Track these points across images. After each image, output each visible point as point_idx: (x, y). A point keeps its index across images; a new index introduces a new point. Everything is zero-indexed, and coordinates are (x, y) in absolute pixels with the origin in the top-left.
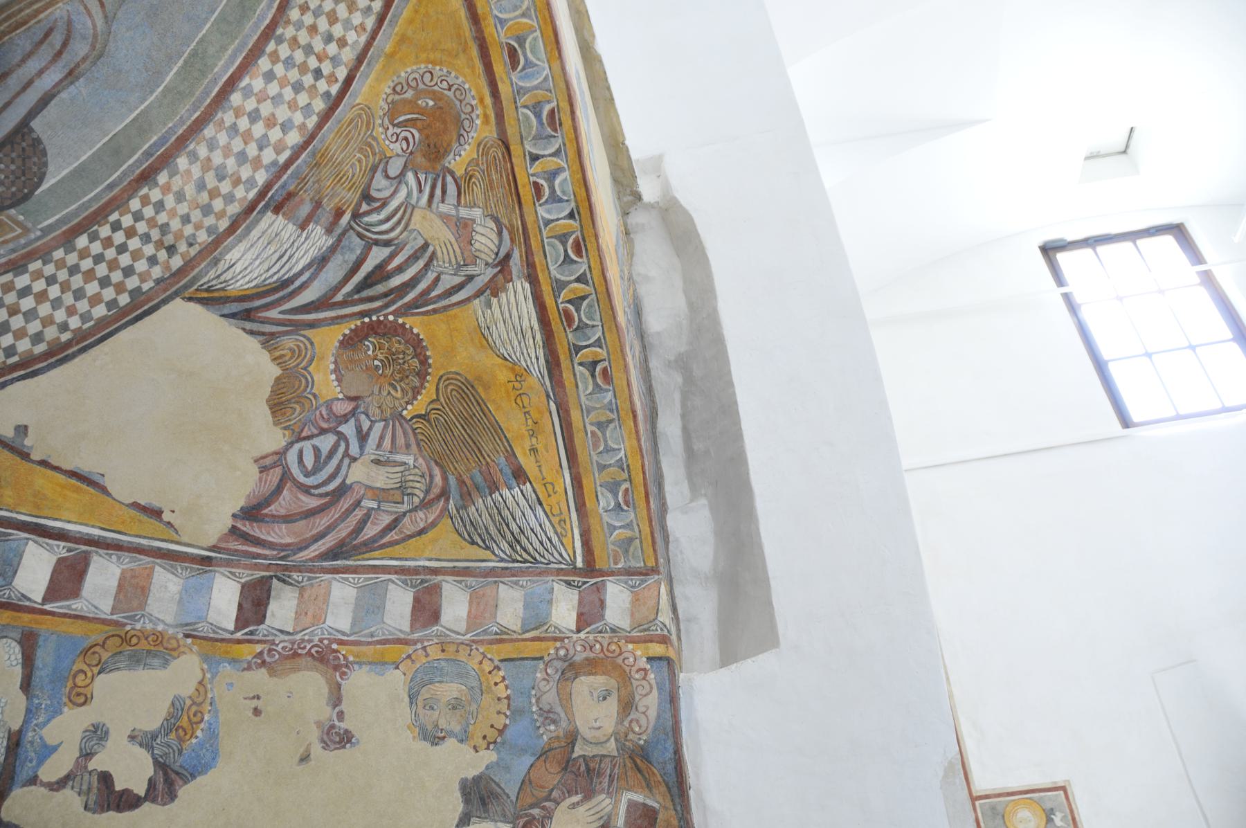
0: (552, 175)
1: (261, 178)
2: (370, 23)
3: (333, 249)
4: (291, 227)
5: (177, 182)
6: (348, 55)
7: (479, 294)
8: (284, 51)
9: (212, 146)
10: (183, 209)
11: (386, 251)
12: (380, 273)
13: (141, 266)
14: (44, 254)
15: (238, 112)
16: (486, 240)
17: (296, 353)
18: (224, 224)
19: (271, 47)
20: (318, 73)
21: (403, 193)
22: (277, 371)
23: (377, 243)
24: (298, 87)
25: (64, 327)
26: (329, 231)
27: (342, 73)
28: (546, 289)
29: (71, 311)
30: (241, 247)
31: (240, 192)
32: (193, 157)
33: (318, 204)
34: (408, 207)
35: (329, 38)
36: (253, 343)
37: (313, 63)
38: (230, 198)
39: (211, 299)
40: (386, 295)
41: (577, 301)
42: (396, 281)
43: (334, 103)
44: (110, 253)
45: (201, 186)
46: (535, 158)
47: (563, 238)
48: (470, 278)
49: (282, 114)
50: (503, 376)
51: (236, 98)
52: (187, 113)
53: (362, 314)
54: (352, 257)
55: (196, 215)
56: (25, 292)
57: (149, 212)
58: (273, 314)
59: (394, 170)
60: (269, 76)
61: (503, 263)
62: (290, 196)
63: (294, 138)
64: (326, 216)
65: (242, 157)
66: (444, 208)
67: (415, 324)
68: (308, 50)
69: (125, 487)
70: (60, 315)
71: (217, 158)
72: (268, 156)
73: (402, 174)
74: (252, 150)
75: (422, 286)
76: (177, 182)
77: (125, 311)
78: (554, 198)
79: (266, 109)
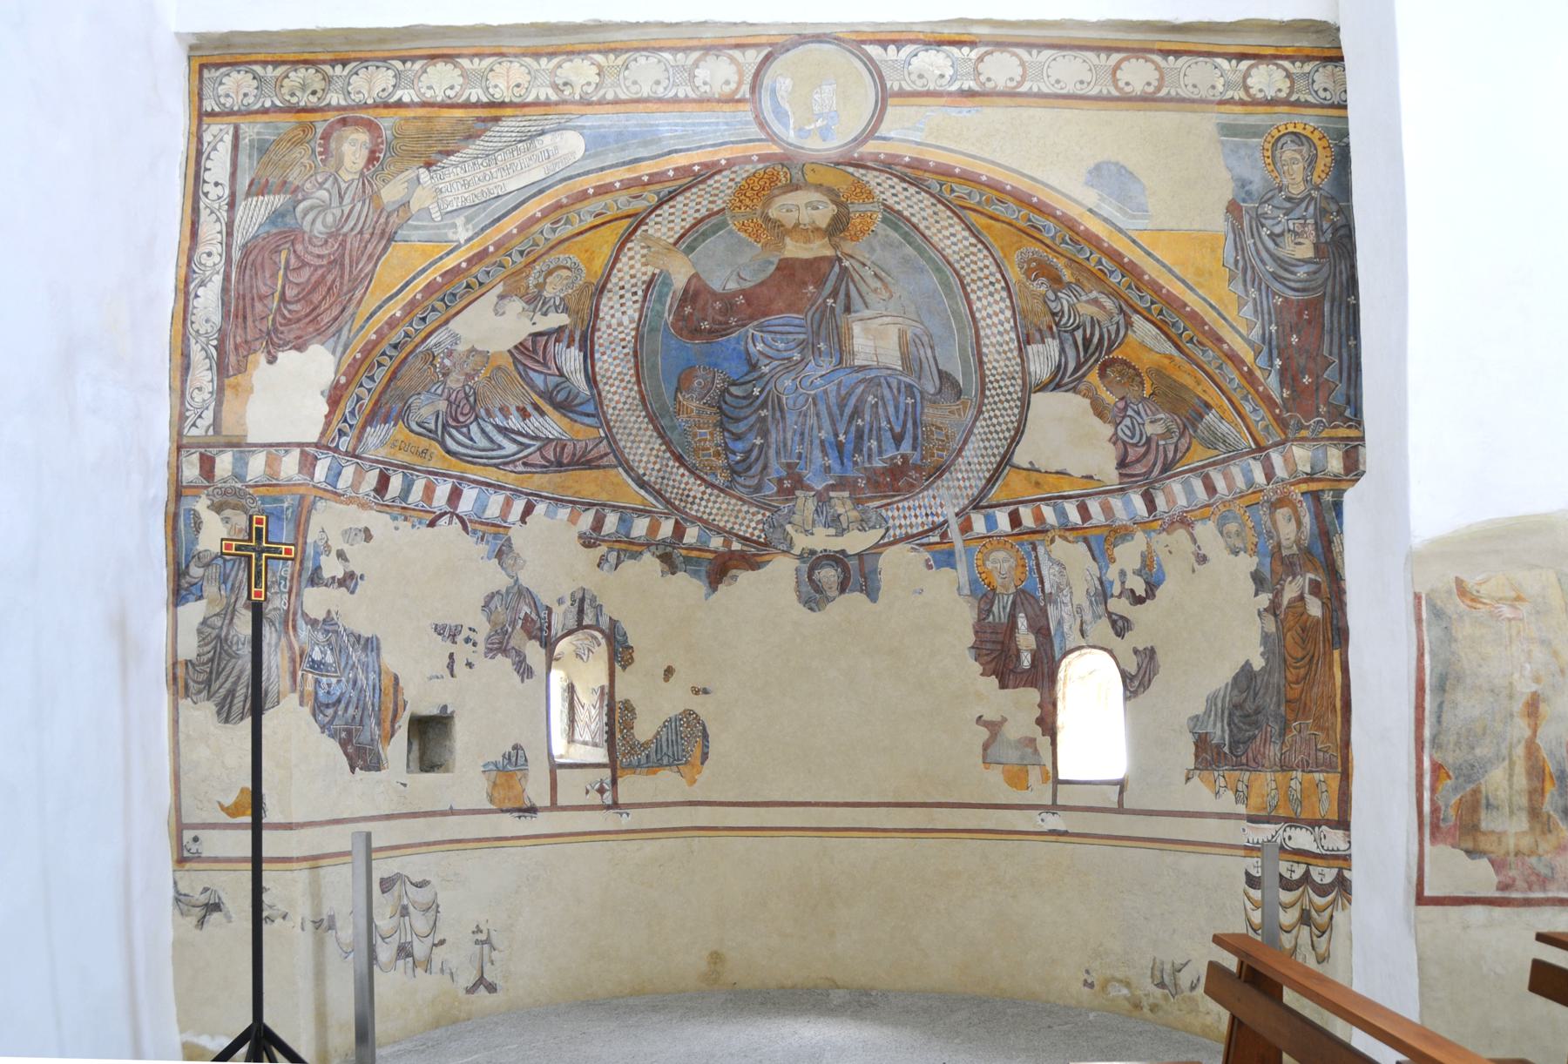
0: (1099, 262)
1: (1013, 335)
2: (985, 252)
3: (1061, 343)
4: (1040, 346)
5: (990, 357)
6: (993, 268)
7: (1127, 329)
8: (974, 287)
9: (988, 338)
10: (1002, 363)
11: (1081, 331)
12: (1087, 342)
13: (1011, 389)
14: (982, 404)
15: (984, 319)
16: (1108, 304)
17: (1088, 390)
18: (1019, 360)
19: (969, 290)
20: (991, 283)
21: (1065, 303)
22: (1088, 401)
23: (1074, 330)
24: (991, 294)
25: (1012, 422)
26: (1053, 338)
27: (999, 276)
28: (1146, 314)
29: (1009, 416)
30: (1032, 364)
31: (1012, 346)
32: (986, 345)
33: (1040, 331)
34: (1071, 306)
35: (981, 270)
36: (1070, 395)
37: (986, 282)
38: (1011, 350)
39: (1042, 387)
40: (1096, 349)
41: (1161, 313)
42: (1095, 340)
43: (1007, 288)
44: (999, 391)
45: (999, 353)
46: (1088, 259)
47: (1129, 287)
48: (1118, 323)
49: (996, 308)
50: (1166, 361)
51: (978, 315)
52: (970, 332)
53: (1096, 361)
54: (1071, 341)
55: (1008, 363)
56: (990, 418)
57: (994, 372)
58: (1066, 380)
59: (1053, 298)
60: (979, 299)
61: (1121, 310)
62: (1028, 335)
63: (1008, 313)
64: (1048, 333)
65: (1000, 333)
66: (1084, 298)
67: (1117, 354)
68: (980, 279)
69: (1077, 472)
70: (1007, 419)
71: (994, 341)
72: (1007, 326)
73: (1057, 296)
74: (1001, 329)
75: (1106, 336)
76: (990, 357)
77: (1022, 406)
78: (1112, 272)
79: (990, 311)
